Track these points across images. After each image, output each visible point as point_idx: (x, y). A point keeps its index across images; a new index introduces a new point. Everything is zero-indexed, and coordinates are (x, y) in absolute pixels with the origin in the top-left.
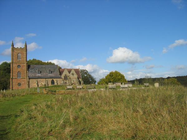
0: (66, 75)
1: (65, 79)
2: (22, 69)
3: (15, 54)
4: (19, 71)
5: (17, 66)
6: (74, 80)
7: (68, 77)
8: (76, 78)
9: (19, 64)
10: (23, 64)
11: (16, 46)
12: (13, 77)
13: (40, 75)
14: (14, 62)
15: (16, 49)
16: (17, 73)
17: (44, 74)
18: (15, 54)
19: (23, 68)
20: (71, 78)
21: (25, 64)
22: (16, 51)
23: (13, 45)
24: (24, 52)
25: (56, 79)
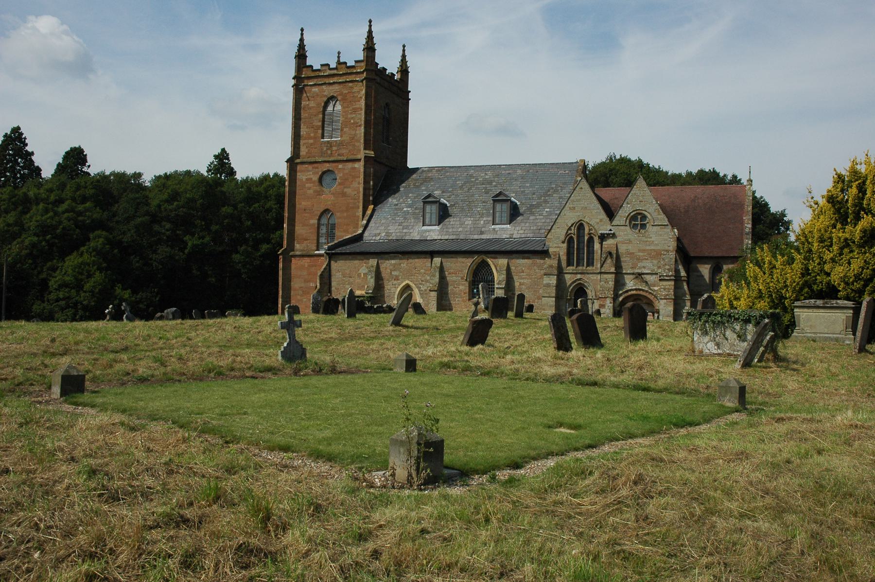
0: (580, 226)
1: (569, 263)
2: (344, 194)
3: (312, 104)
4: (326, 211)
5: (316, 178)
6: (647, 266)
7: (597, 246)
8: (658, 255)
9: (327, 166)
10: (349, 165)
11: (314, 61)
12: (297, 246)
13: (434, 232)
14: (303, 151)
15: (316, 75)
16: (314, 221)
17: (462, 224)
18: (311, 104)
19: (348, 191)
20: (622, 249)
21: (356, 165)
22: (315, 90)
23: (301, 56)
24: (355, 89)
25: (503, 262)
